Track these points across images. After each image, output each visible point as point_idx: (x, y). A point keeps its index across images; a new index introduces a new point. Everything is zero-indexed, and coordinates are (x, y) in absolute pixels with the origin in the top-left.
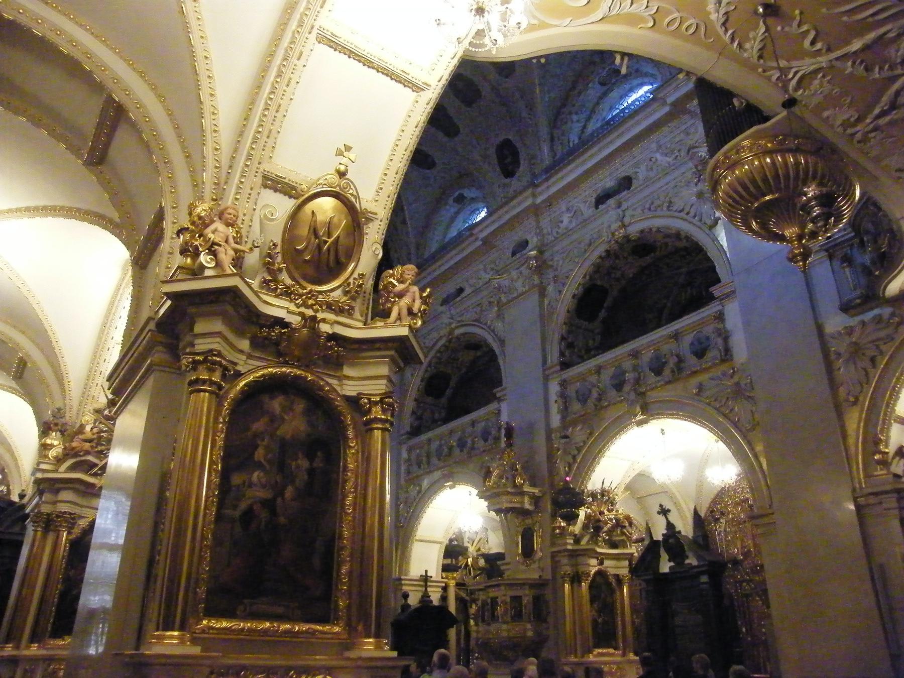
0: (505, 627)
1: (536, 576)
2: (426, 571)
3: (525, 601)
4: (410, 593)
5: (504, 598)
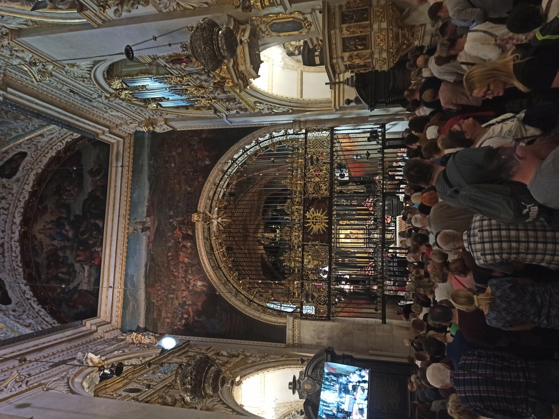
0: (376, 56)
1: (320, 16)
2: (326, 84)
3: (346, 34)
4: (346, 98)
5: (346, 59)
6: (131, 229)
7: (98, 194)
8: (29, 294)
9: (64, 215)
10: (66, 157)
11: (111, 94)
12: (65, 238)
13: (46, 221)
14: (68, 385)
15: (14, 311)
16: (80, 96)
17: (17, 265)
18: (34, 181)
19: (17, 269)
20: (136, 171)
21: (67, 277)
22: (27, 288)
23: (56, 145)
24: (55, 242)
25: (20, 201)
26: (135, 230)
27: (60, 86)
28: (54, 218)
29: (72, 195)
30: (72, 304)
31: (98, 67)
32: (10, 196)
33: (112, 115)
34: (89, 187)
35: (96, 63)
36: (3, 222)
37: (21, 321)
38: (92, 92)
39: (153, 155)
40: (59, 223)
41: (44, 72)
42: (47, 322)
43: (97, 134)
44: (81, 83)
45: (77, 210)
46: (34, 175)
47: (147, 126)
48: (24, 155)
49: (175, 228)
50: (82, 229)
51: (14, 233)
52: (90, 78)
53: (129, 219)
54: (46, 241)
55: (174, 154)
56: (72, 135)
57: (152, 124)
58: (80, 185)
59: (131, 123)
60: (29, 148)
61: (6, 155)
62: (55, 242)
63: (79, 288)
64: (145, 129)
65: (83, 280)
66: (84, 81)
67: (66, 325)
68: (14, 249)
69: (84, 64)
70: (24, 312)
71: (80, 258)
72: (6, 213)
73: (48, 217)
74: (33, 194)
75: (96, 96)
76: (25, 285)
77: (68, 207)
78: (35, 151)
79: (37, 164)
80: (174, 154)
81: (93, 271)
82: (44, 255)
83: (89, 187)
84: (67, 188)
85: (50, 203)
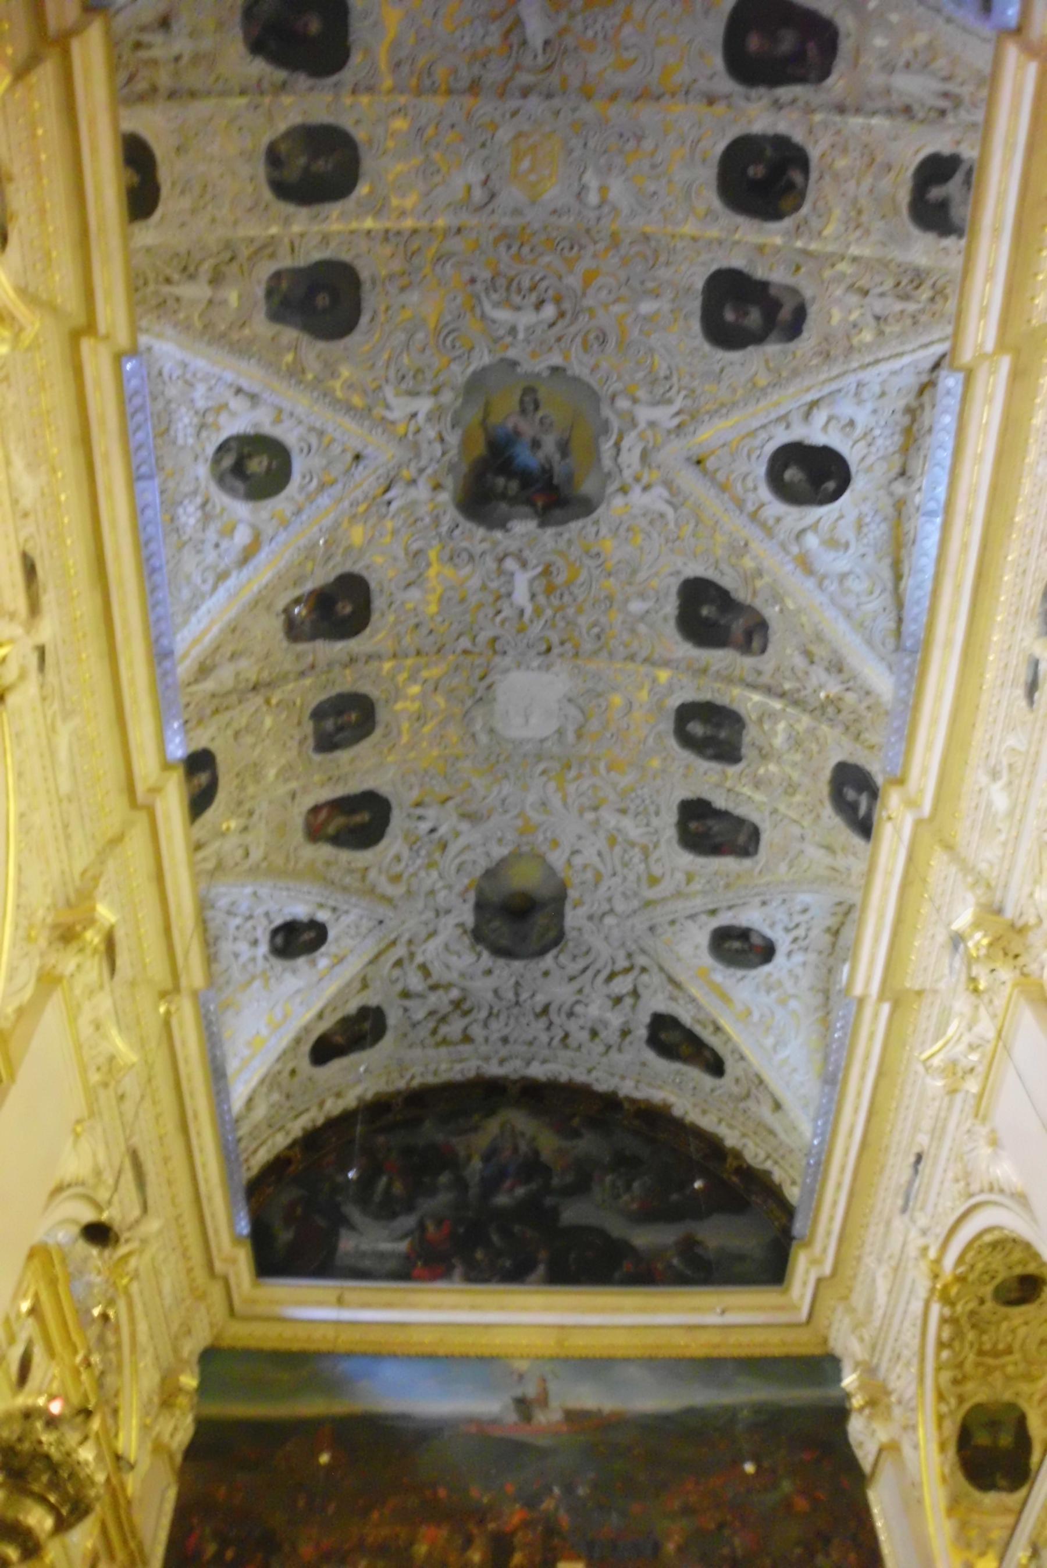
6: (523, 1365)
7: (627, 1266)
8: (334, 1107)
9: (555, 1181)
10: (725, 1176)
11: (938, 1261)
12: (491, 1184)
13: (534, 1139)
14: (76, 1184)
15: (293, 1072)
16: (911, 1183)
17: (413, 1077)
18: (647, 1102)
19: (402, 1077)
20: (712, 1368)
21: (377, 1197)
22: (350, 1100)
23: (757, 1145)
24: (476, 1164)
25: (589, 1071)
26: (521, 1377)
27: (926, 1124)
28: (546, 1155)
29: (618, 1197)
30: (299, 1211)
31: (1007, 1207)
32: (601, 1049)
33: (874, 1281)
34: (644, 1238)
35: (1021, 1199)
36: (530, 1037)
37: (264, 1089)
38: (930, 1208)
39: (771, 1422)
40: (533, 1167)
41: (954, 1074)
42: (255, 1151)
43: (808, 1243)
44: (950, 1175)
45: (573, 1213)
46: (664, 1100)
47: (862, 1387)
48: (716, 1067)
49: (531, 1502)
50: (517, 1228)
51: (502, 1062)
52: (971, 1195)
53: (553, 1359)
54: (482, 1140)
55: (786, 1486)
56: (794, 1183)
57: (871, 1403)
58: (650, 1214)
59: (861, 1339)
60: (737, 1081)
61: (711, 1028)
62: (476, 1164)
63: (344, 1232)
64: (849, 1380)
65: (367, 1238)
66: (957, 1180)
67: (241, 1196)
68: (458, 1067)
69: (1004, 1171)
70: (288, 1097)
71: (431, 1228)
72: (556, 1042)
73: (548, 1143)
74: (611, 1102)
75: (923, 1221)
76: (360, 1099)
77: (581, 1186)
78: (730, 1096)
79: (695, 1105)
80: (786, 1486)
81: (391, 1265)
82: (440, 1138)
83: (644, 1238)
84: (636, 1185)
85: (588, 1144)
